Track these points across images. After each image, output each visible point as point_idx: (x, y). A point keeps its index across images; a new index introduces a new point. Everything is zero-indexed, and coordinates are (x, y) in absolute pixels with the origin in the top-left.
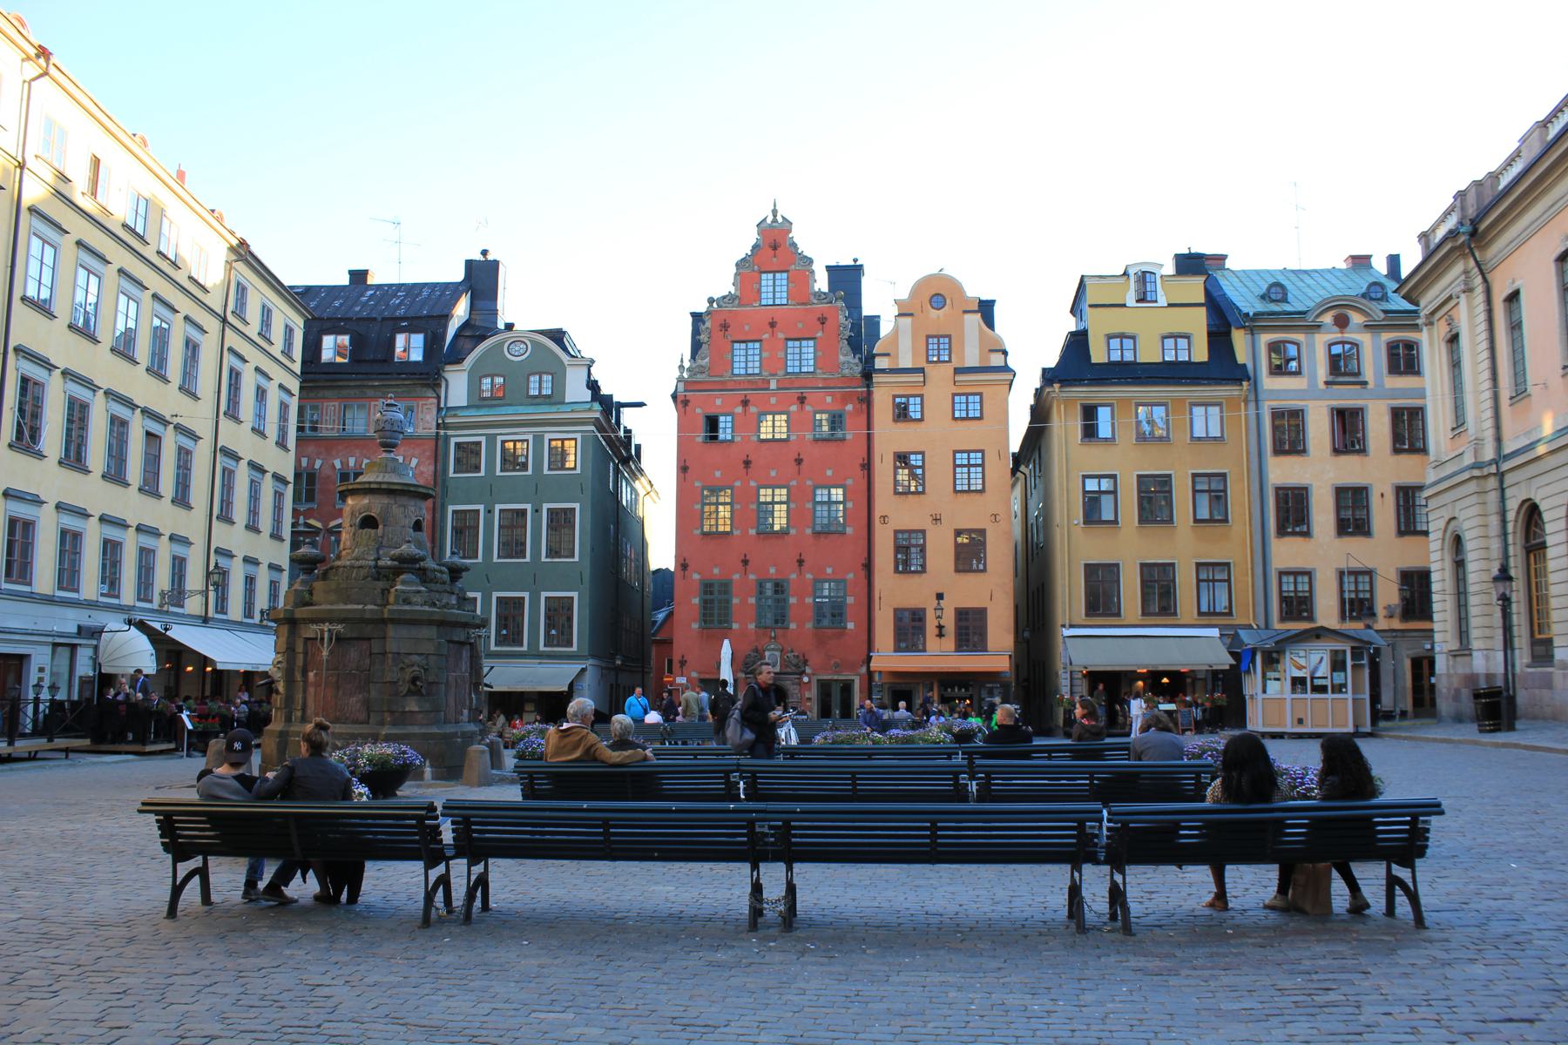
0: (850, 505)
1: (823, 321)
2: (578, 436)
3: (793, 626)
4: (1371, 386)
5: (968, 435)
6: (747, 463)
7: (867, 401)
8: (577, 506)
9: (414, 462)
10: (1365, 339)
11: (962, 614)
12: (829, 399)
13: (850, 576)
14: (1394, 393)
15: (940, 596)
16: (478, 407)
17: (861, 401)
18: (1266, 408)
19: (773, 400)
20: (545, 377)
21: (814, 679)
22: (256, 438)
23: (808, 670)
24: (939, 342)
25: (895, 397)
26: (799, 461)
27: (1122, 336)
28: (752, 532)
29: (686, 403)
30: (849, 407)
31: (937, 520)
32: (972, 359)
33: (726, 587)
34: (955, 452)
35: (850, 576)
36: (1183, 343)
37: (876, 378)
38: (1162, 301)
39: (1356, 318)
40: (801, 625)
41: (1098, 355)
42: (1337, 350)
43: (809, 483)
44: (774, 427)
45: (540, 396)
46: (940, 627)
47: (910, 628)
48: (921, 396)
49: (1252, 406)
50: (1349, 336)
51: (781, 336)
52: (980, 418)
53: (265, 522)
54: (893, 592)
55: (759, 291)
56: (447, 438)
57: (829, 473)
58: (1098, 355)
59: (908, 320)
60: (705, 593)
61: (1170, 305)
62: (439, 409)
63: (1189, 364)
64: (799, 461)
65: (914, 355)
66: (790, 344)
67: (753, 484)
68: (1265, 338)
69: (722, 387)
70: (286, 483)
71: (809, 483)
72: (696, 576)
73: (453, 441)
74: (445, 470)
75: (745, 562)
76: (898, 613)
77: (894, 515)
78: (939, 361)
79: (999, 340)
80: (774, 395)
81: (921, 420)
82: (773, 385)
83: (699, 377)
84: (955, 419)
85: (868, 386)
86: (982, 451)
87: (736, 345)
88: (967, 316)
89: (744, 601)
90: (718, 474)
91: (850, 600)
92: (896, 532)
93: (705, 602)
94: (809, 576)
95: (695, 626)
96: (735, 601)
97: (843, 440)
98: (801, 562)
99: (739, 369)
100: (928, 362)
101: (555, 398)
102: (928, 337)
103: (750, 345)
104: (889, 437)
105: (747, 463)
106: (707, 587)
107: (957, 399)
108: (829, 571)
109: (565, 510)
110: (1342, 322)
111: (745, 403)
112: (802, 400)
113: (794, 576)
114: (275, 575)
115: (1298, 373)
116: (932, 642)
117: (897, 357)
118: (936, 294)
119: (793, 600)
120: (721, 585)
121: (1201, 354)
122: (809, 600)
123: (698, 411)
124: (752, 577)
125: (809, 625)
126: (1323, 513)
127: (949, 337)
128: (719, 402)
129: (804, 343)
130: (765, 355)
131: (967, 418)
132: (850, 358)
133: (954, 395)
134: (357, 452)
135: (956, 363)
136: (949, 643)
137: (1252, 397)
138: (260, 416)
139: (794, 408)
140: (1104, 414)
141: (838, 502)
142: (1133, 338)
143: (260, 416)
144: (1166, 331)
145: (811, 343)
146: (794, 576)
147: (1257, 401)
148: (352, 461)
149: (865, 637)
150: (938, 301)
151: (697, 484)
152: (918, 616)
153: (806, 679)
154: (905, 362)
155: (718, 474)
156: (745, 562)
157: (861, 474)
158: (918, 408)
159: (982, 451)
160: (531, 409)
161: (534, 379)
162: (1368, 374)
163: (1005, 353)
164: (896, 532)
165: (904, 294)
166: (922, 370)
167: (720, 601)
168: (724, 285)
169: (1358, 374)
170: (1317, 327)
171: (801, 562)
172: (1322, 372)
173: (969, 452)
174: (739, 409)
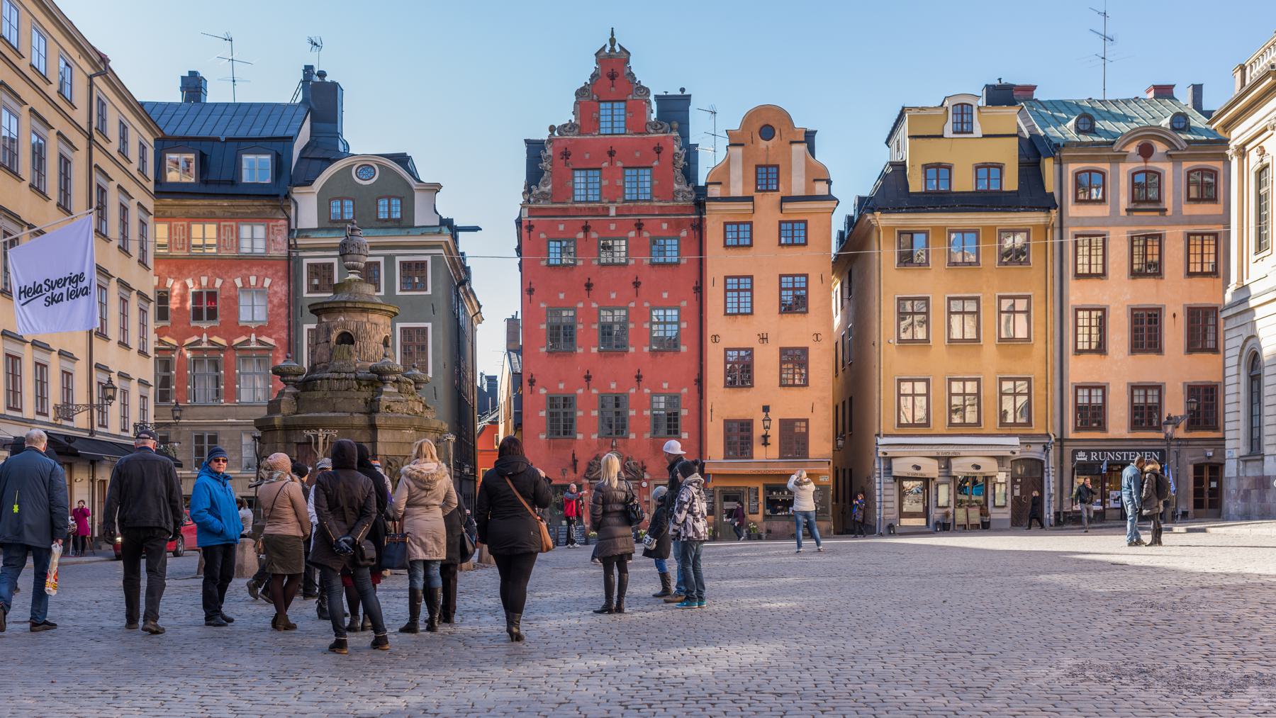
0: (684, 325)
1: (658, 150)
2: (428, 259)
3: (632, 436)
4: (1169, 213)
5: (795, 260)
6: (589, 286)
7: (699, 228)
8: (429, 325)
9: (267, 282)
10: (1167, 168)
11: (787, 425)
12: (665, 226)
13: (685, 390)
14: (1191, 220)
15: (766, 409)
16: (329, 230)
17: (693, 227)
19: (613, 227)
20: (393, 202)
21: (652, 483)
22: (123, 256)
23: (647, 476)
24: (767, 176)
25: (726, 224)
26: (637, 284)
27: (938, 166)
28: (594, 350)
29: (530, 228)
30: (684, 234)
31: (764, 339)
32: (798, 188)
33: (568, 401)
34: (781, 276)
35: (685, 390)
36: (995, 173)
37: (710, 206)
38: (978, 131)
39: (1160, 148)
40: (639, 435)
41: (916, 184)
42: (1141, 178)
43: (647, 304)
45: (390, 219)
46: (765, 437)
47: (740, 436)
48: (751, 223)
49: (1057, 232)
50: (1153, 165)
51: (619, 164)
52: (806, 244)
53: (134, 341)
54: (723, 404)
55: (598, 121)
56: (299, 260)
57: (665, 295)
58: (916, 184)
59: (739, 150)
60: (551, 406)
61: (984, 136)
62: (290, 231)
63: (1001, 192)
64: (637, 284)
65: (745, 184)
66: (628, 172)
67: (594, 305)
68: (1071, 168)
69: (565, 213)
70: (148, 300)
71: (647, 304)
72: (543, 391)
73: (305, 262)
74: (298, 289)
75: (588, 378)
76: (728, 423)
77: (725, 334)
78: (767, 190)
79: (825, 170)
80: (613, 221)
81: (751, 245)
82: (613, 212)
83: (542, 204)
84: (780, 244)
85: (701, 214)
86: (806, 276)
87: (577, 173)
88: (795, 147)
89: (587, 414)
90: (562, 296)
91: (684, 412)
92: (726, 350)
93: (551, 414)
94: (647, 391)
95: (543, 437)
96: (580, 413)
97: (677, 264)
98: (639, 378)
99: (579, 194)
100: (757, 191)
101: (404, 223)
102: (757, 167)
103: (590, 173)
104: (720, 264)
105: (589, 286)
106: (552, 401)
107: (784, 226)
108: (665, 385)
109: (418, 329)
110: (1146, 151)
111: (586, 229)
112: (639, 226)
113: (633, 391)
114: (144, 389)
115: (1103, 201)
116: (759, 452)
117: (728, 186)
118: (766, 126)
119: (632, 413)
120: (565, 399)
121: (1011, 182)
122: (647, 413)
123: (543, 236)
124: (594, 391)
125: (647, 436)
127: (777, 166)
128: (561, 227)
129: (641, 172)
130: (605, 183)
131: (793, 244)
132: (683, 187)
133: (780, 222)
134: (210, 272)
135: (783, 191)
136: (773, 451)
137: (1057, 225)
138: (125, 237)
140: (919, 240)
141: (671, 323)
142: (949, 168)
143: (125, 237)
144: (980, 160)
145: (648, 172)
146: (633, 391)
147: (1061, 228)
148: (204, 281)
149: (696, 446)
150: (767, 132)
151: (542, 305)
152: (746, 425)
153: (644, 484)
154: (737, 190)
155: (562, 296)
156: (588, 378)
157: (693, 296)
158: (748, 234)
159: (806, 276)
160: (381, 232)
161: (383, 203)
162: (1168, 202)
163: (829, 182)
164: (726, 350)
165: (736, 125)
166: (751, 199)
167: (565, 414)
168: (565, 114)
169: (1159, 200)
170: (1122, 158)
171: (639, 378)
172: (1124, 201)
173: (793, 276)
174: (581, 235)
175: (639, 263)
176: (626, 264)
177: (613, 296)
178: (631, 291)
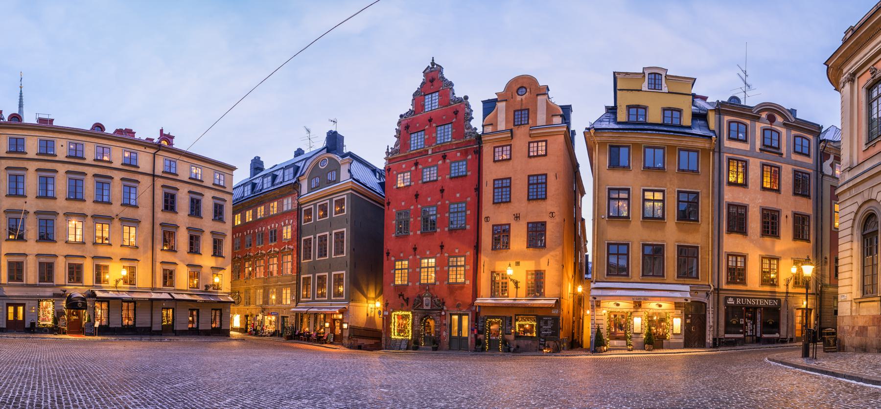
1: (456, 113)
18: (725, 156)
19: (430, 160)
23: (445, 308)
26: (442, 191)
28: (419, 232)
44: (430, 174)
64: (442, 191)
75: (415, 249)
112: (444, 157)
126: (754, 223)
137: (717, 150)
139: (440, 162)
147: (720, 152)
153: (443, 313)
156: (415, 249)
175: (444, 179)
176: (436, 181)
177: (429, 199)
178: (439, 195)
